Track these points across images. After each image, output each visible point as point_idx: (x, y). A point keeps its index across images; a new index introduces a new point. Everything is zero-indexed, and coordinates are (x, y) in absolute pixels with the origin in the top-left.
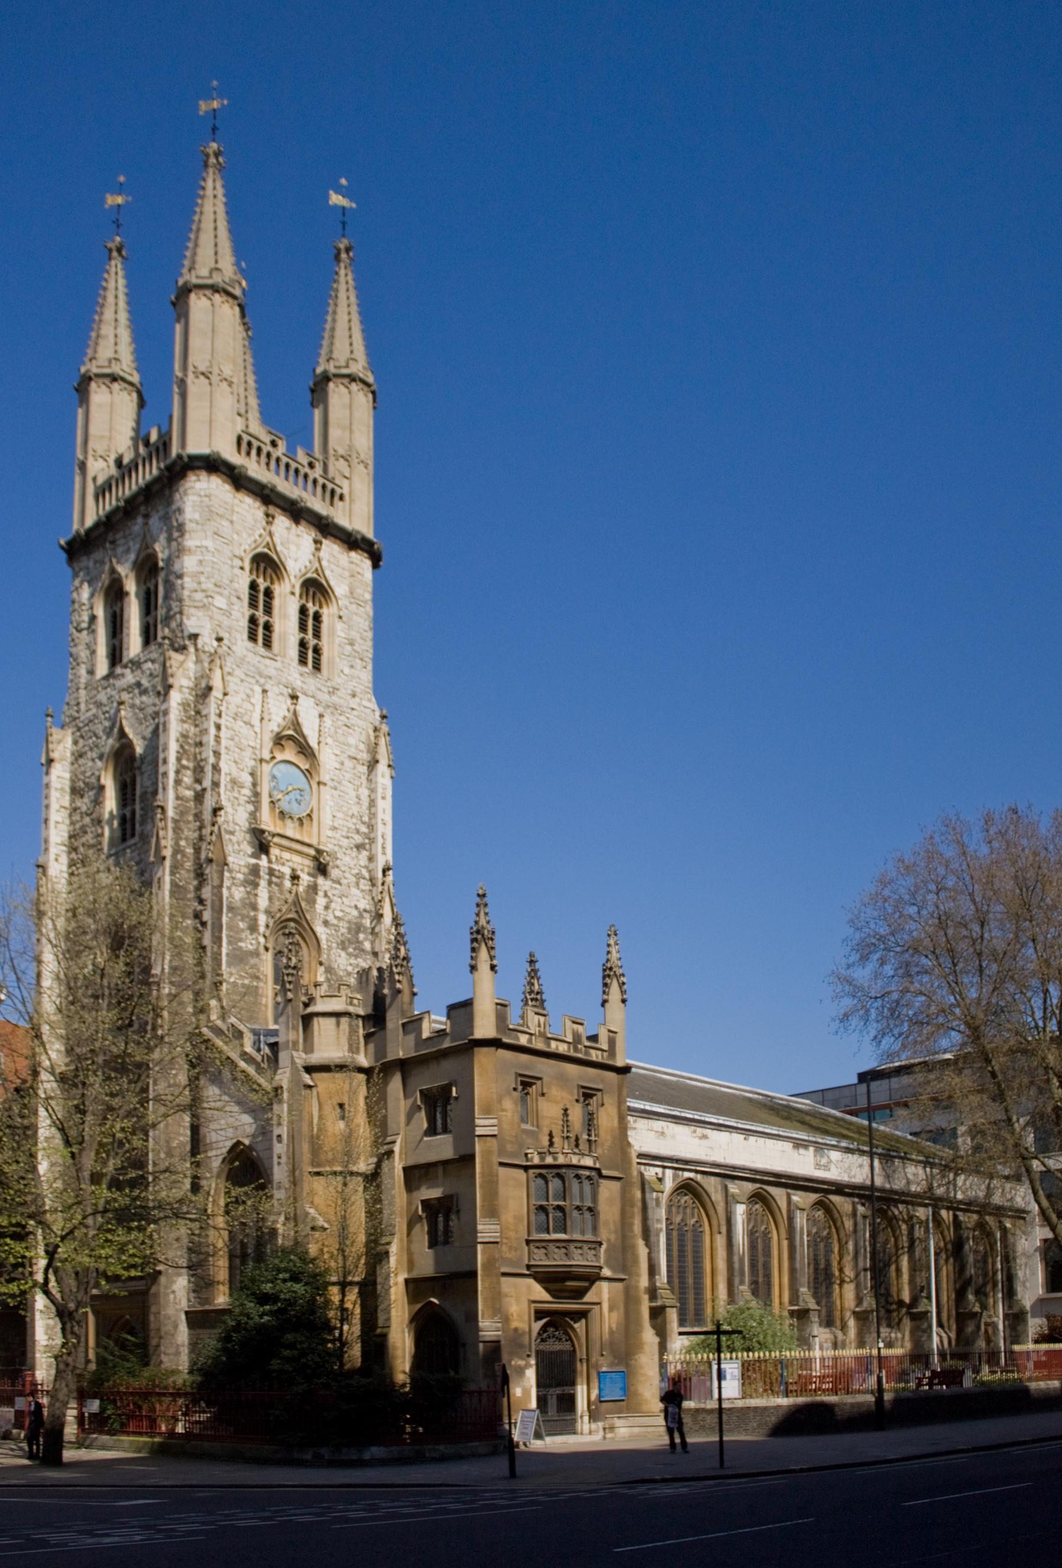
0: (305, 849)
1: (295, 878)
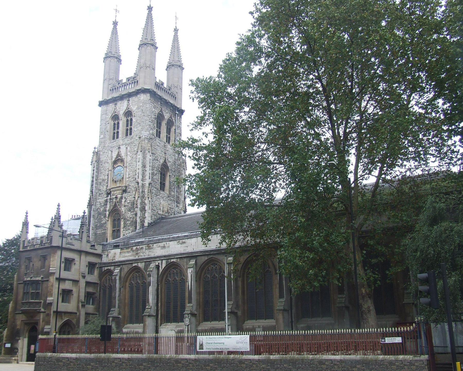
0: (119, 188)
1: (116, 198)
